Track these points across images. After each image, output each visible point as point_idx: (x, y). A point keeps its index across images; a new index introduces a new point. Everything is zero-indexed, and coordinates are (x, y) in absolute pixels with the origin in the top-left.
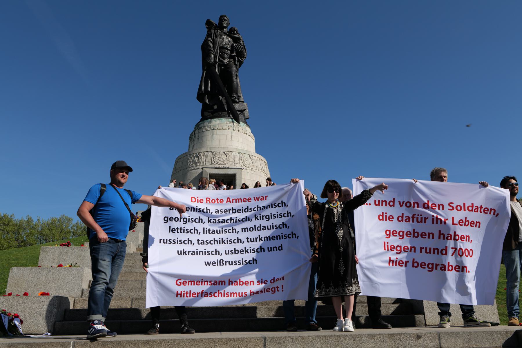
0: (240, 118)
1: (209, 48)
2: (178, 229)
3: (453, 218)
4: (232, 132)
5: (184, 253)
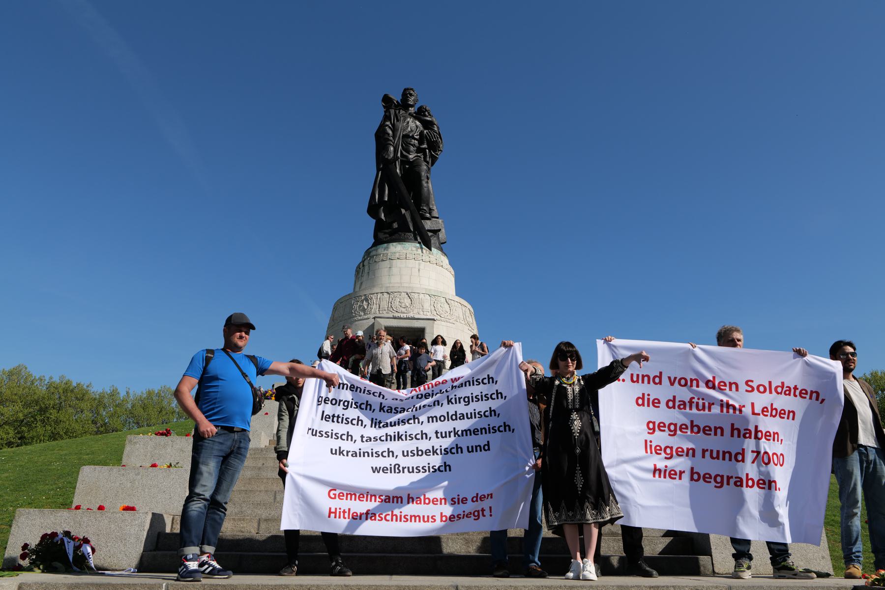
0: (432, 241)
1: (386, 136)
2: (334, 416)
3: (753, 404)
4: (419, 264)
5: (341, 453)
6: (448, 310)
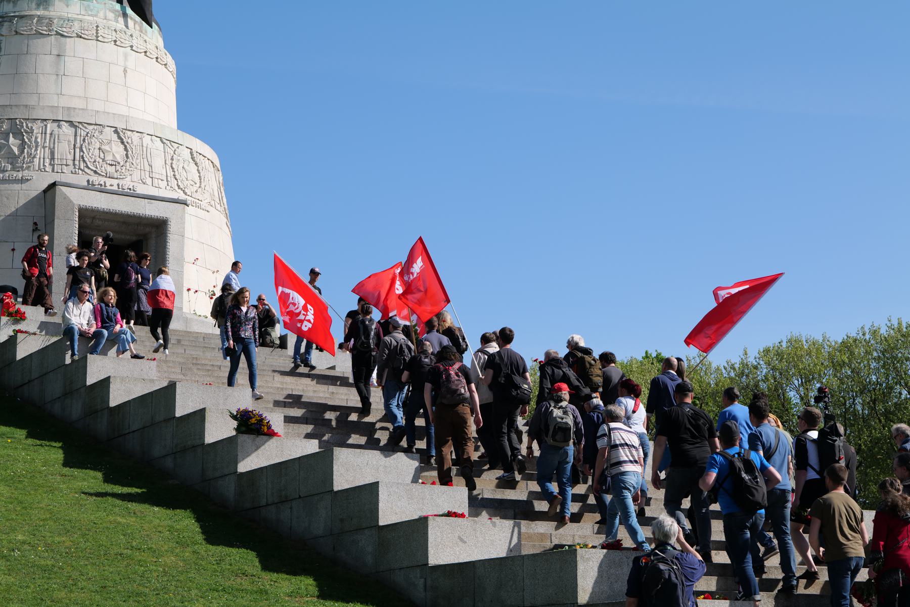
4: (126, 56)
6: (197, 180)
